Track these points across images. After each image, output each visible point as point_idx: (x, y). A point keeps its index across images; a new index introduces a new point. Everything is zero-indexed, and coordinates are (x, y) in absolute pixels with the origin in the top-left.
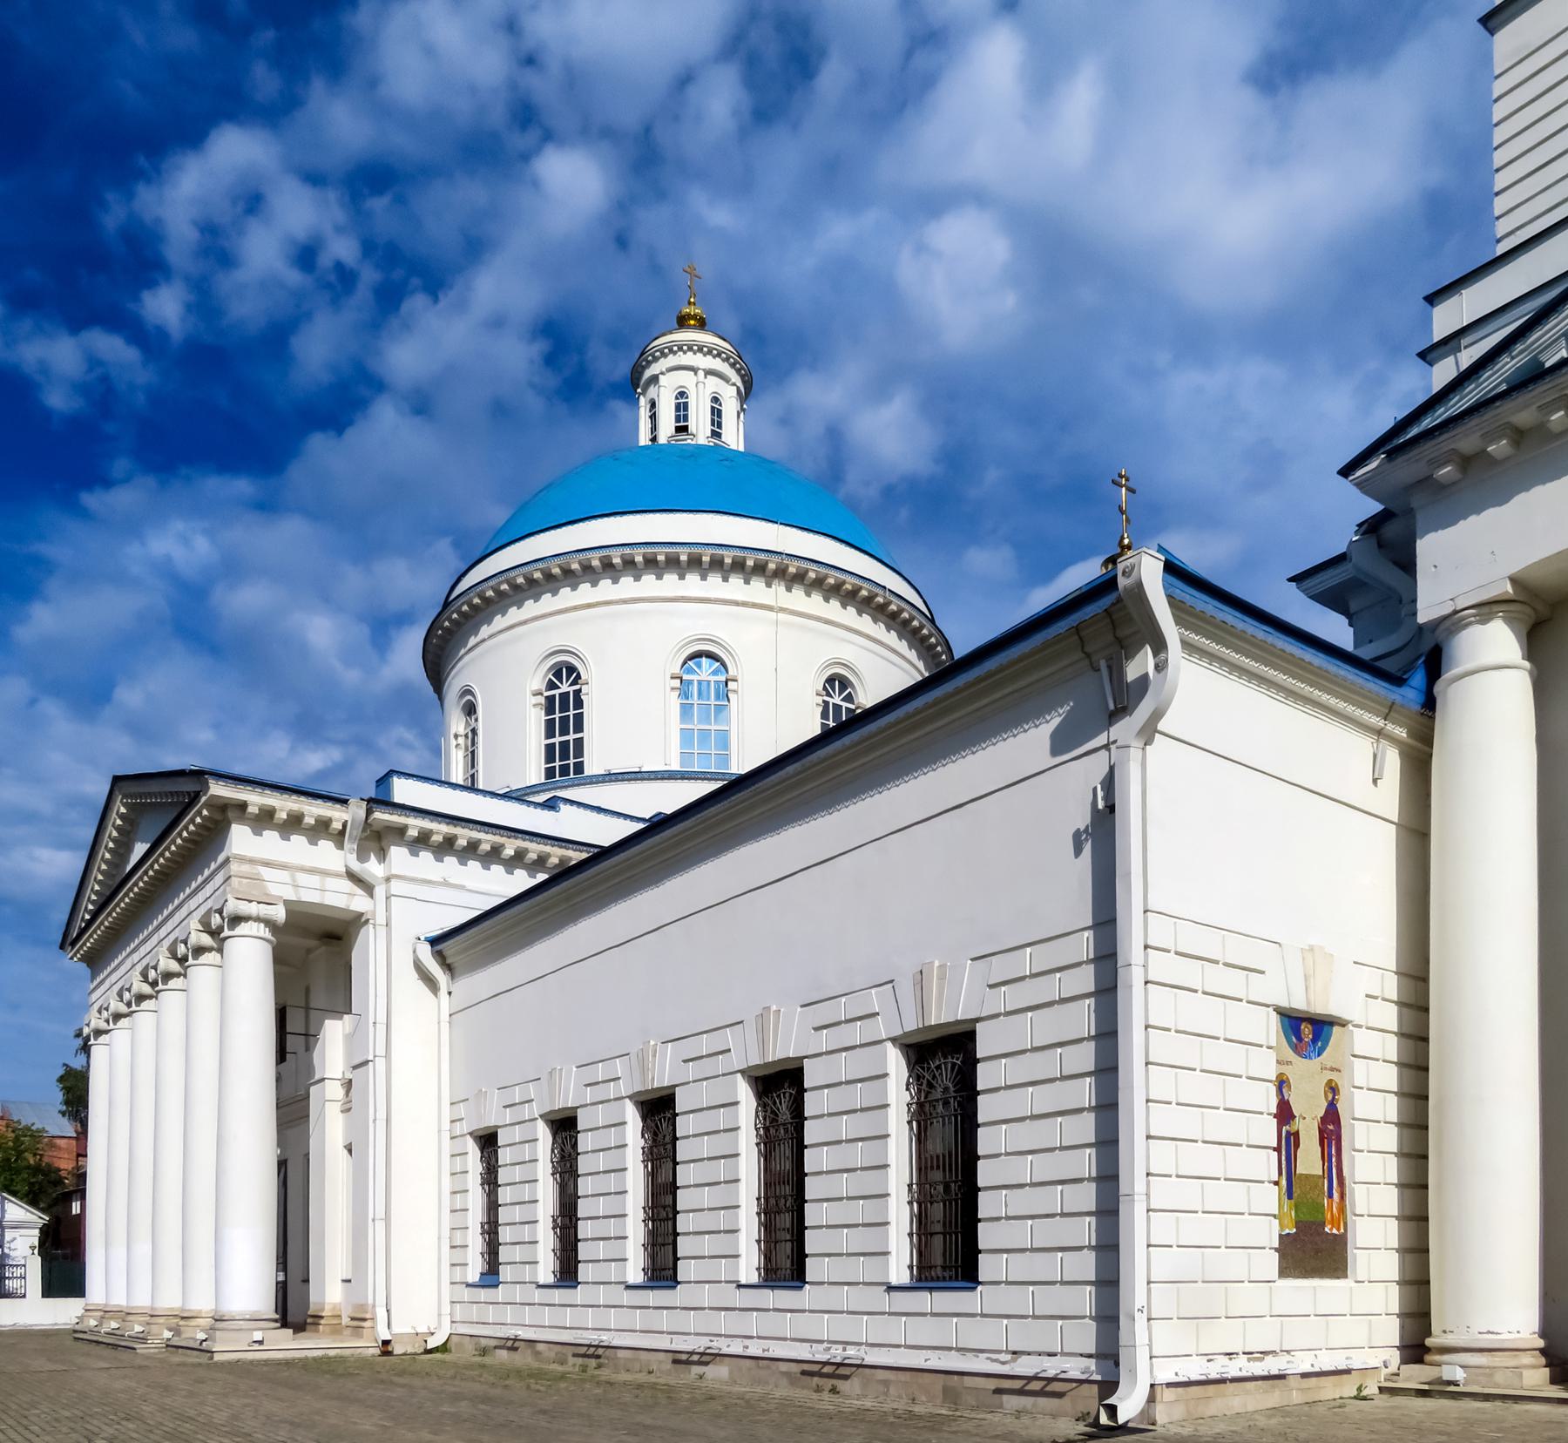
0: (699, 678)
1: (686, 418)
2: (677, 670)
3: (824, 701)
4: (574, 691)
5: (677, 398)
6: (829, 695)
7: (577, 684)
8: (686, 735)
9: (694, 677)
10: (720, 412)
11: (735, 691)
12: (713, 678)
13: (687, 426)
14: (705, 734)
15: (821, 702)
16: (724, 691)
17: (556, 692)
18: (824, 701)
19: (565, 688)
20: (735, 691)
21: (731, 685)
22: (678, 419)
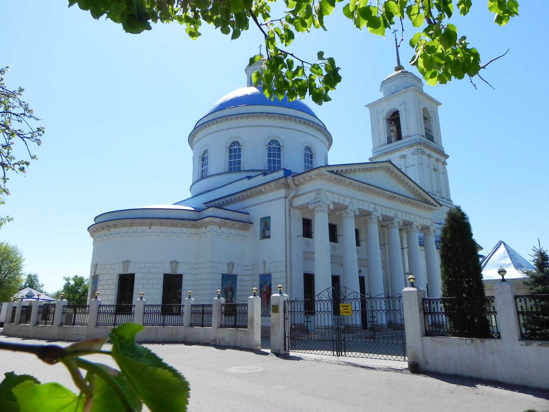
0: (273, 146)
2: (267, 143)
3: (305, 152)
4: (238, 148)
7: (239, 146)
8: (269, 161)
9: (272, 146)
11: (283, 150)
12: (276, 147)
14: (274, 161)
15: (304, 153)
16: (279, 150)
17: (233, 148)
18: (305, 152)
19: (235, 147)
20: (283, 150)
21: (281, 148)
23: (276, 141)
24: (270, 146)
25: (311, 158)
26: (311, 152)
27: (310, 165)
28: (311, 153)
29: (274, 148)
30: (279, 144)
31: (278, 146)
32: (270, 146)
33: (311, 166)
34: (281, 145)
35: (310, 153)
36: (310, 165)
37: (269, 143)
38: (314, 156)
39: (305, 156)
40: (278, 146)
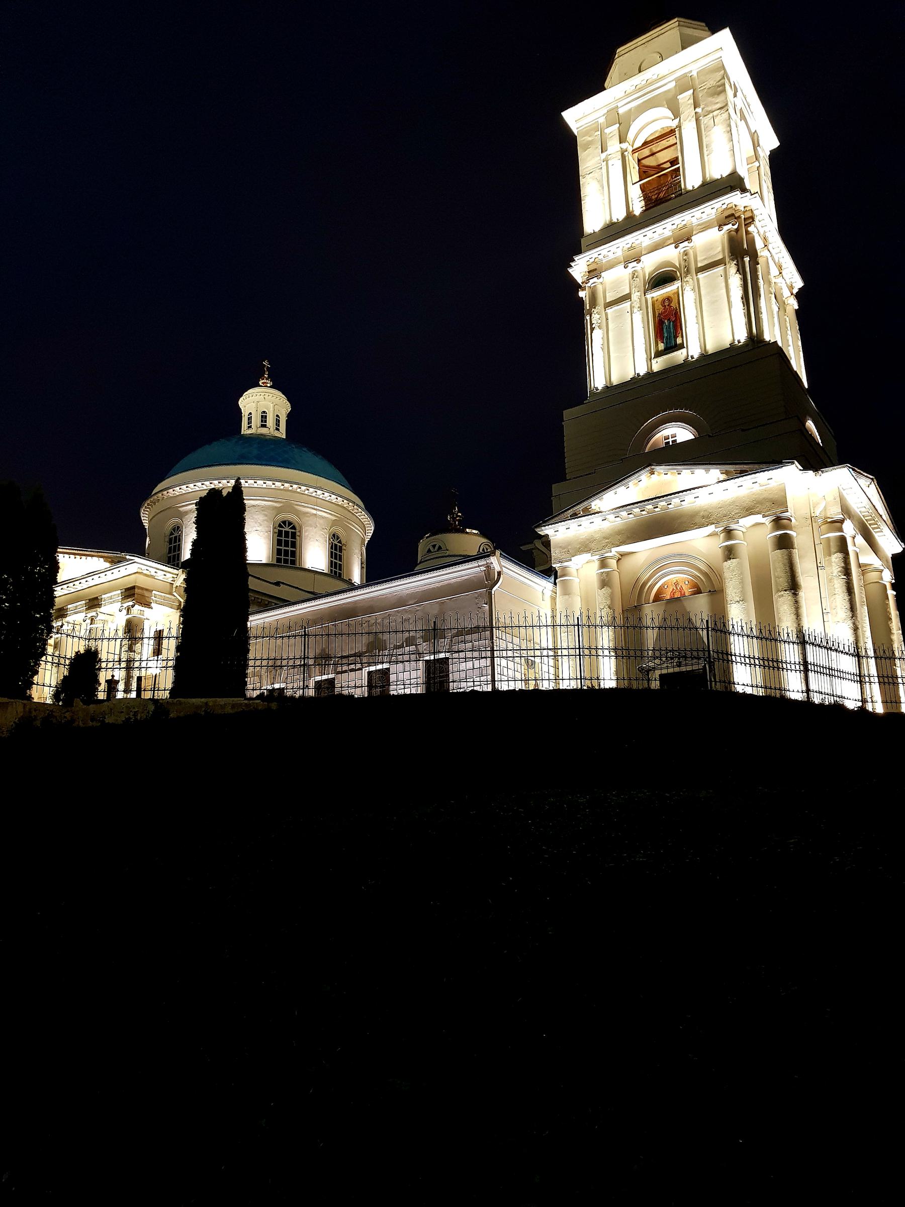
1: (266, 422)
5: (262, 413)
6: (333, 540)
10: (279, 420)
13: (266, 425)
14: (286, 552)
22: (262, 421)
23: (290, 524)
24: (281, 529)
25: (341, 551)
26: (340, 542)
27: (338, 562)
28: (341, 544)
29: (287, 533)
30: (294, 528)
31: (293, 531)
32: (281, 529)
33: (340, 563)
34: (297, 528)
35: (338, 544)
36: (338, 562)
37: (280, 526)
38: (344, 547)
39: (332, 548)
40: (293, 531)
